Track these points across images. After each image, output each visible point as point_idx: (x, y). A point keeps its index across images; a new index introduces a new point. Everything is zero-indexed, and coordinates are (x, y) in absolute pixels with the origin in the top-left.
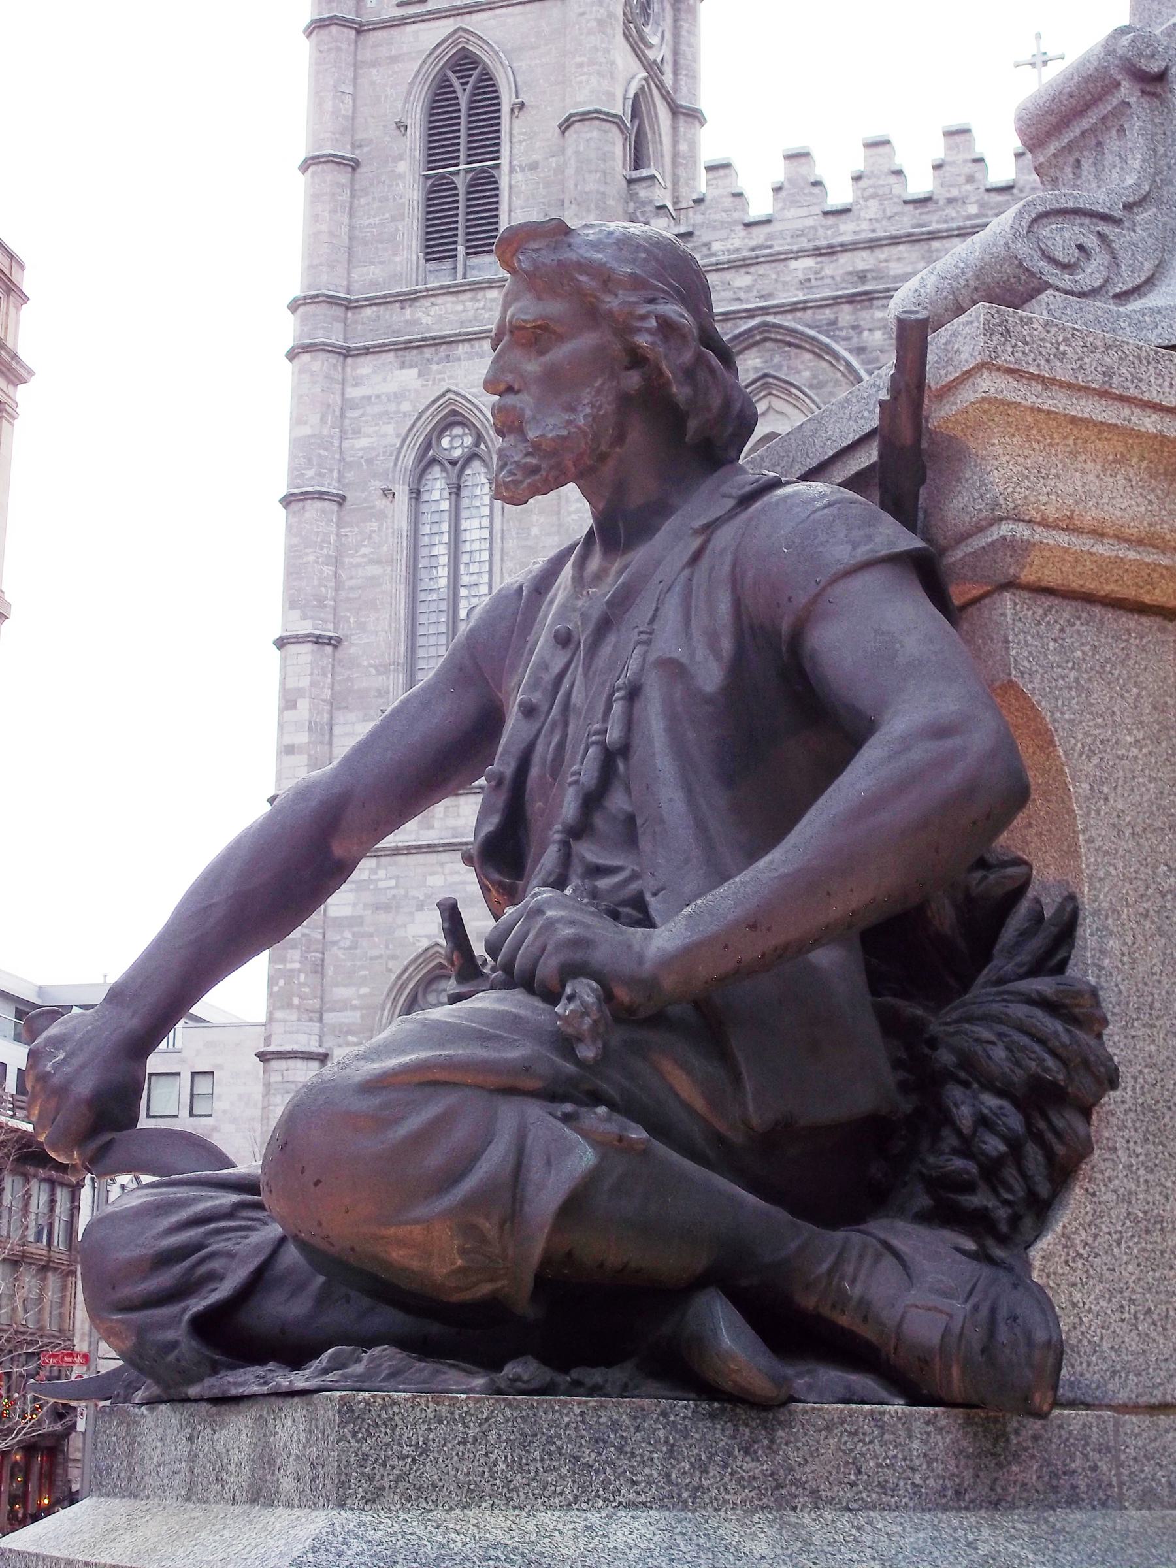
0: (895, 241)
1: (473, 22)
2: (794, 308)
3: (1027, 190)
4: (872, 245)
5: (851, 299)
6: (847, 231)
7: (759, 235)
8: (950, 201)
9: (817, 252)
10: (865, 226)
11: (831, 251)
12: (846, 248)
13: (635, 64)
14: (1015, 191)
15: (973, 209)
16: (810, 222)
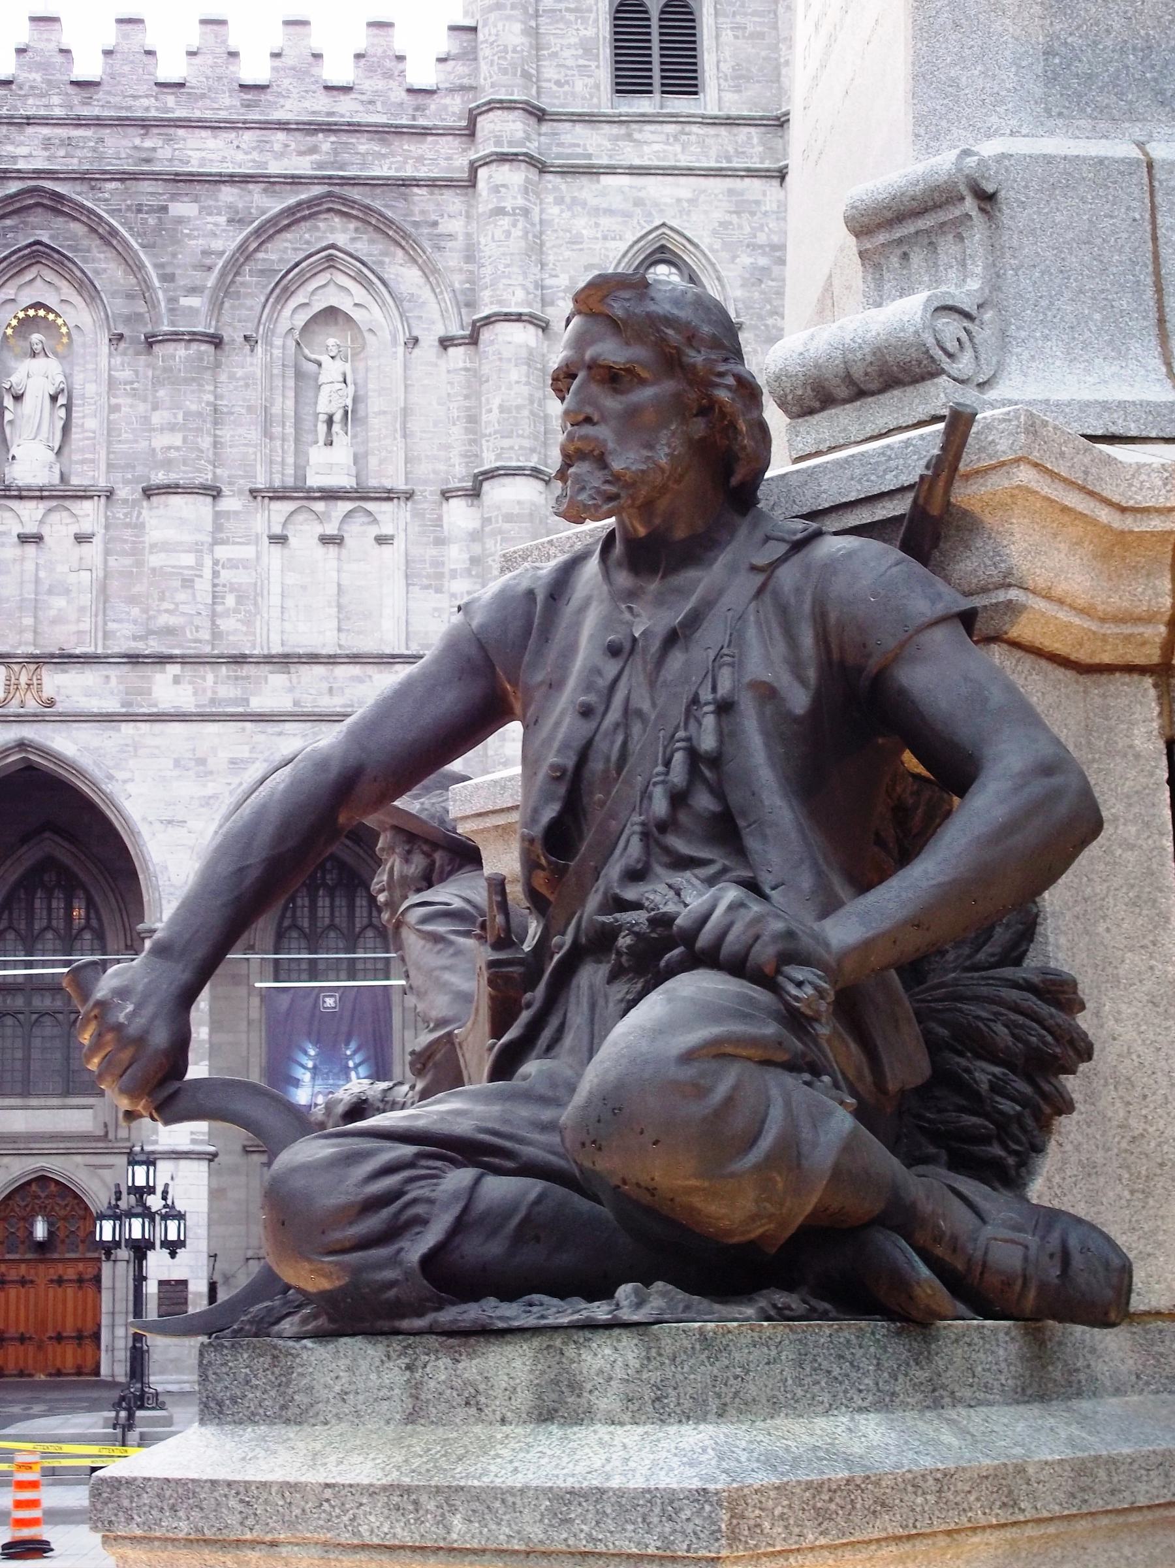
3: (26, 87)
14: (14, 87)
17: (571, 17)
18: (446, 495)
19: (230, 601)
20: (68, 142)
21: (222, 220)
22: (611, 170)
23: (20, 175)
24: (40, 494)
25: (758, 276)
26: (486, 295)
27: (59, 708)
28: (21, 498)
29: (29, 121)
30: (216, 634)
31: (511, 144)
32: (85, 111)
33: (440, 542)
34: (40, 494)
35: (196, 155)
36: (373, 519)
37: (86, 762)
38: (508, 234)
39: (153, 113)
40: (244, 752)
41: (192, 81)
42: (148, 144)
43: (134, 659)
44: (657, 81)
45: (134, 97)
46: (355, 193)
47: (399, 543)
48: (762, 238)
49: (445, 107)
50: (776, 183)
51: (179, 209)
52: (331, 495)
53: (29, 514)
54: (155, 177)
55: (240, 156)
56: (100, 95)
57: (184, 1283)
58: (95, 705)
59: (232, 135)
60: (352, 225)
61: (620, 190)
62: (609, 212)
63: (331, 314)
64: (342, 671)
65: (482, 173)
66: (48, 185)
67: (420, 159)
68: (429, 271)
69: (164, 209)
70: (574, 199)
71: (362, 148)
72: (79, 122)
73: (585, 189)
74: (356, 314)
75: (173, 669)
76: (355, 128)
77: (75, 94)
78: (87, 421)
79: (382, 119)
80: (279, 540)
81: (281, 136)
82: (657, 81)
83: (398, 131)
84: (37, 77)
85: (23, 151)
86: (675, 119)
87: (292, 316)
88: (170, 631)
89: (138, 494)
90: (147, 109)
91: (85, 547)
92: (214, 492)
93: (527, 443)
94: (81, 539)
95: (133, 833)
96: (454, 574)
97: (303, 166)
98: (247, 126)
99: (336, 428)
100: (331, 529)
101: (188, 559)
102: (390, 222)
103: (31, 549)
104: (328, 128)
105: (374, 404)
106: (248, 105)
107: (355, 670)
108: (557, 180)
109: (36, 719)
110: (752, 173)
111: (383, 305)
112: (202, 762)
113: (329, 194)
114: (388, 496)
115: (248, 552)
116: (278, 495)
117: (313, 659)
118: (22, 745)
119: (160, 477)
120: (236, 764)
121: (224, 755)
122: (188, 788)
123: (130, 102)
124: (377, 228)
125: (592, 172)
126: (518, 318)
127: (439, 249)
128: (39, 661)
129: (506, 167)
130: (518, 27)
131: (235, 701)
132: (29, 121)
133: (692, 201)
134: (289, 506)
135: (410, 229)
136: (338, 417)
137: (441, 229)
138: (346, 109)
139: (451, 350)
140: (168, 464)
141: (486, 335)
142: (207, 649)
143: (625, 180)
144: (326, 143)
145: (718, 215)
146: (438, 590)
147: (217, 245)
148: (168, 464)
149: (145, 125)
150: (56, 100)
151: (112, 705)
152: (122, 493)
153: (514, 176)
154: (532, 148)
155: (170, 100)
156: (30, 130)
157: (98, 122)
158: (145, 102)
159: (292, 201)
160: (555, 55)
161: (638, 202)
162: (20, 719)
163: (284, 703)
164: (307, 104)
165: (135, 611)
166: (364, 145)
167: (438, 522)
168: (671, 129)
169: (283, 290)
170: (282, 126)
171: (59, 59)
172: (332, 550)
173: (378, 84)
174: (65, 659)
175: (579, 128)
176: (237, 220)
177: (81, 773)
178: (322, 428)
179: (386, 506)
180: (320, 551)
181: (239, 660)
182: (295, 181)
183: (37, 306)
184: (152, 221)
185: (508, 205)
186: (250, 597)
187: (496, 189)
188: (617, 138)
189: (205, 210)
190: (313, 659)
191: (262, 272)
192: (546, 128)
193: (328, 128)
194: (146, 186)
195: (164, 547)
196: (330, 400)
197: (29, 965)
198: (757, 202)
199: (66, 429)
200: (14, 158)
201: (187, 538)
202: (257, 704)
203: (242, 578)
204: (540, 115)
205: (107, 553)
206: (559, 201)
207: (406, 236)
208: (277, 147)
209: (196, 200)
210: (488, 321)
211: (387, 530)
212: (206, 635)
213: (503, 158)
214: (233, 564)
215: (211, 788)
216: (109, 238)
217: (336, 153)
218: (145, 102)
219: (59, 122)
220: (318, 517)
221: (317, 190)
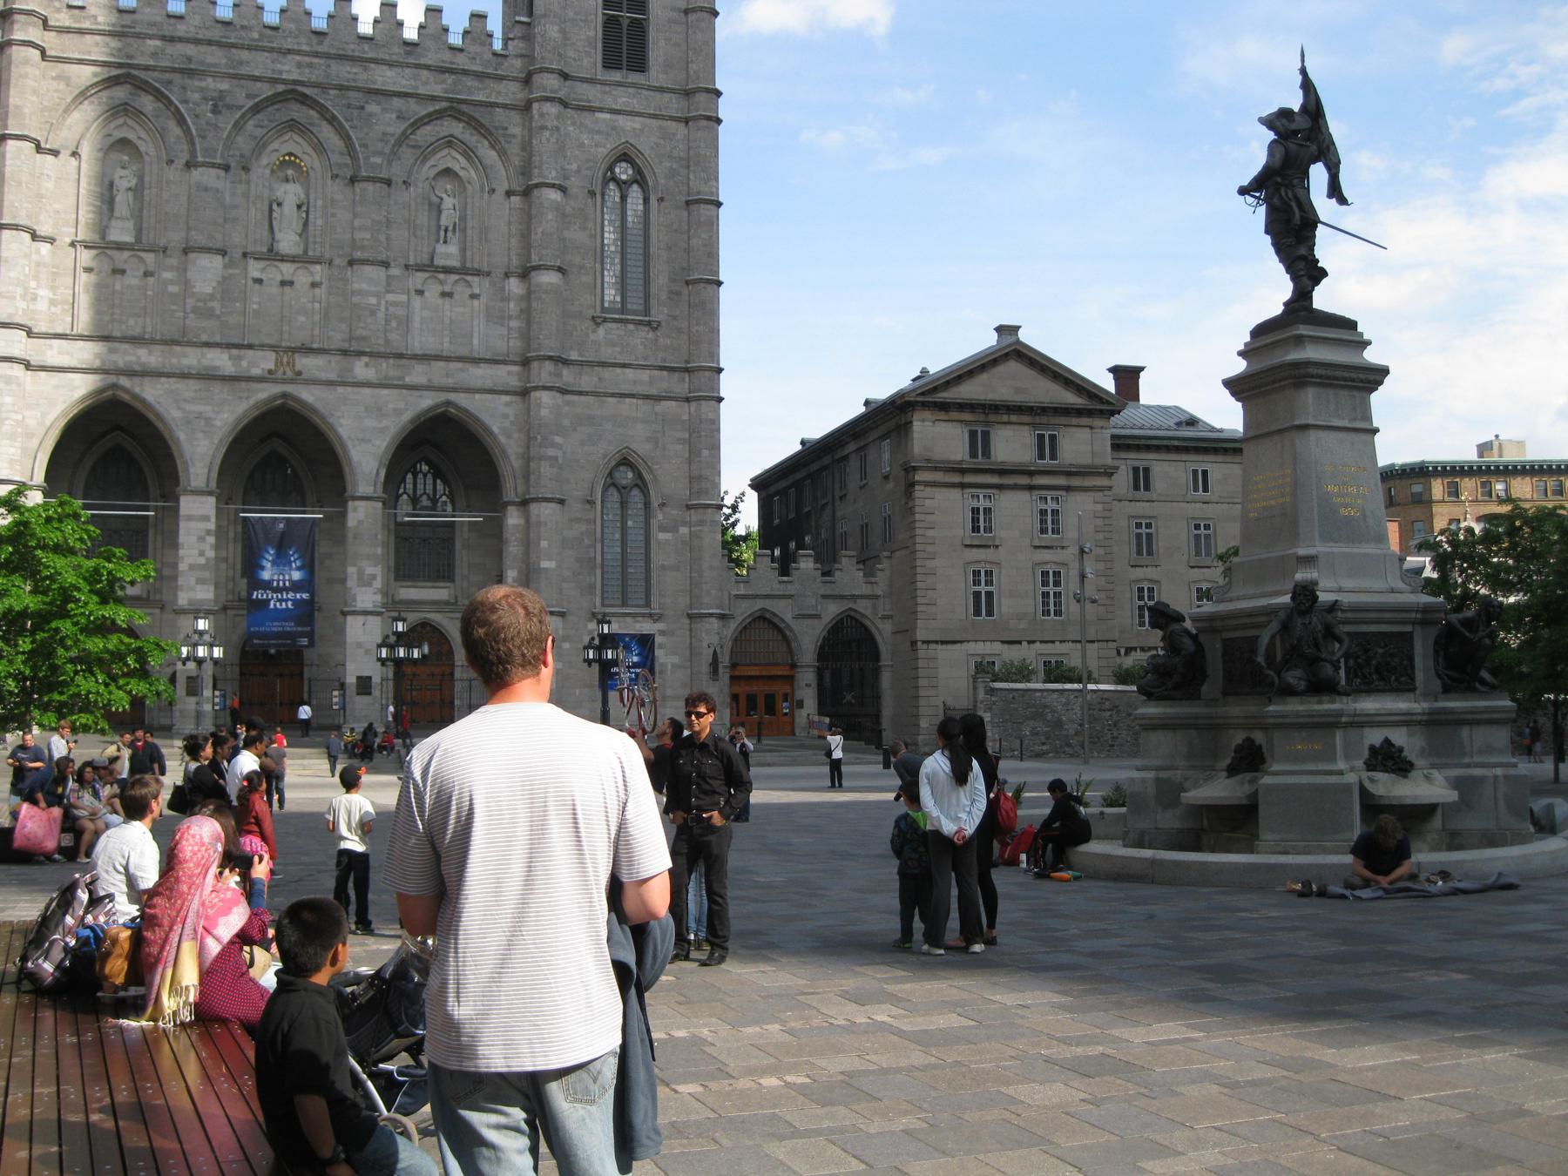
0: (210, 43)
2: (147, 68)
4: (197, 42)
5: (182, 71)
6: (181, 29)
7: (128, 19)
8: (243, 27)
9: (164, 38)
10: (192, 29)
11: (171, 40)
12: (181, 40)
15: (256, 36)
16: (159, 19)
17: (582, 24)
18: (507, 275)
19: (394, 324)
20: (310, 65)
21: (394, 116)
22: (601, 110)
23: (284, 82)
24: (293, 259)
25: (673, 173)
26: (536, 171)
27: (305, 376)
28: (282, 261)
29: (290, 52)
30: (387, 341)
31: (551, 92)
32: (320, 49)
34: (293, 259)
35: (380, 79)
36: (469, 285)
37: (318, 405)
38: (548, 140)
39: (357, 54)
40: (401, 405)
41: (378, 37)
42: (354, 70)
43: (345, 353)
44: (625, 63)
45: (347, 43)
46: (465, 108)
47: (484, 299)
48: (675, 153)
49: (513, 66)
50: (683, 124)
51: (372, 108)
52: (448, 270)
53: (287, 269)
54: (358, 89)
55: (404, 82)
56: (327, 41)
57: (370, 678)
58: (324, 376)
59: (400, 70)
60: (461, 125)
61: (605, 120)
62: (599, 132)
63: (447, 172)
64: (454, 365)
65: (535, 105)
66: (300, 88)
67: (499, 93)
68: (502, 154)
69: (363, 108)
70: (581, 124)
71: (469, 84)
72: (316, 55)
73: (587, 118)
74: (462, 173)
75: (365, 359)
76: (465, 72)
77: (314, 39)
78: (317, 220)
79: (480, 69)
80: (420, 292)
81: (425, 73)
82: (625, 63)
83: (488, 76)
84: (292, 26)
85: (286, 68)
86: (634, 85)
87: (427, 171)
88: (364, 339)
89: (345, 263)
90: (353, 51)
91: (317, 291)
92: (386, 264)
93: (556, 253)
95: (343, 446)
96: (510, 317)
97: (437, 89)
98: (408, 65)
99: (450, 234)
100: (447, 289)
101: (373, 300)
102: (483, 126)
103: (287, 289)
104: (451, 71)
106: (408, 53)
107: (461, 365)
108: (573, 112)
109: (292, 381)
110: (672, 118)
111: (476, 170)
112: (380, 409)
113: (452, 108)
114: (478, 273)
115: (404, 298)
116: (420, 268)
117: (438, 358)
118: (285, 395)
119: (358, 254)
120: (398, 412)
121: (391, 406)
122: (371, 423)
123: (345, 46)
124: (475, 128)
126: (553, 186)
127: (509, 142)
128: (294, 350)
129: (548, 104)
130: (556, 28)
131: (399, 379)
132: (290, 52)
133: (642, 130)
134: (426, 275)
135: (493, 131)
136: (451, 228)
137: (509, 132)
138: (461, 61)
139: (513, 198)
140: (362, 248)
141: (536, 192)
142: (382, 349)
143: (607, 116)
144: (450, 79)
145: (653, 139)
146: (502, 325)
147: (390, 130)
148: (362, 248)
149: (352, 59)
150: (303, 40)
151: (332, 376)
152: (337, 261)
153: (551, 109)
154: (561, 94)
155: (366, 47)
156: (290, 57)
157: (327, 56)
158: (352, 46)
159: (431, 109)
160: (573, 44)
161: (614, 128)
162: (284, 381)
163: (423, 380)
164: (439, 56)
165: (344, 326)
166: (470, 82)
167: (503, 289)
168: (631, 90)
169: (424, 156)
170: (427, 67)
171: (304, 18)
172: (447, 300)
173: (477, 48)
174: (307, 350)
175: (585, 85)
176: (401, 117)
177: (316, 411)
178: (442, 233)
179: (476, 279)
180: (440, 301)
181: (400, 356)
182: (433, 98)
183: (290, 154)
184: (356, 113)
185: (549, 124)
186: (406, 322)
187: (542, 115)
188: (605, 93)
189: (385, 110)
190: (438, 358)
191: (414, 147)
192: (568, 83)
193: (451, 71)
194: (352, 94)
195: (360, 292)
197: (304, 513)
198: (674, 134)
199: (306, 224)
200: (281, 72)
201: (373, 289)
202: (408, 380)
203: (401, 312)
204: (565, 76)
205: (329, 293)
206: (573, 124)
207: (491, 134)
208: (424, 79)
209: (379, 104)
210: (537, 186)
211: (477, 291)
212: (381, 342)
213: (548, 99)
214: (395, 304)
215: (385, 423)
216: (332, 120)
217: (455, 83)
218: (352, 46)
219: (306, 54)
220: (441, 282)
221: (445, 104)
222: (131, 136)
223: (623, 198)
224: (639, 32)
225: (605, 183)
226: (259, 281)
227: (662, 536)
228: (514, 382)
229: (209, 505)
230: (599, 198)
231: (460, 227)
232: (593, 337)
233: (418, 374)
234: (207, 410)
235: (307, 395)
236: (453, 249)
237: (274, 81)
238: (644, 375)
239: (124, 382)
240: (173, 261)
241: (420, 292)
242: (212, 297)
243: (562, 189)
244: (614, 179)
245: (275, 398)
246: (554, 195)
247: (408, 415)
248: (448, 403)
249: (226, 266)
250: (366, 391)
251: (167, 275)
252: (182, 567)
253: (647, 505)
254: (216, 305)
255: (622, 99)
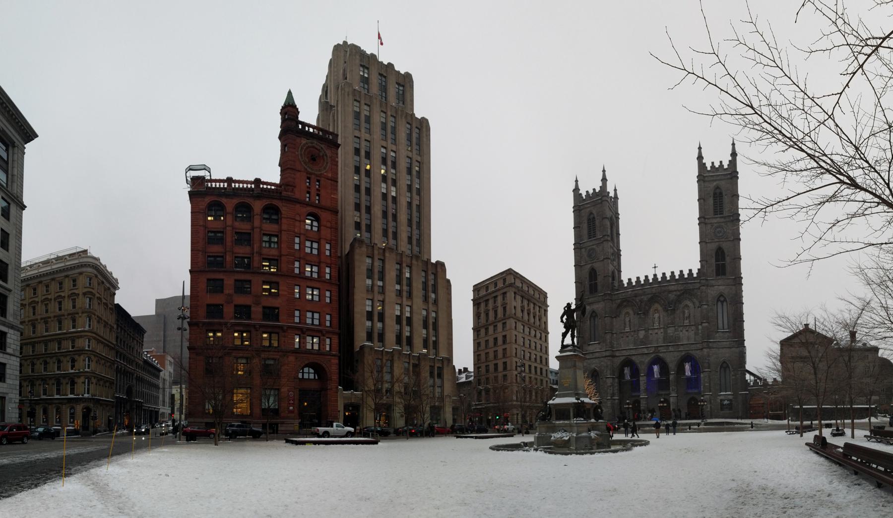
1: (593, 264)
13: (612, 267)
33: (698, 330)
36: (691, 328)
53: (656, 331)
63: (686, 305)
80: (682, 331)
92: (675, 327)
94: (662, 333)
97: (682, 288)
101: (672, 334)
105: (691, 315)
114: (693, 325)
115: (678, 333)
120: (678, 356)
125: (713, 286)
143: (717, 287)
162: (657, 353)
176: (675, 295)
182: (681, 290)
195: (669, 333)
196: (686, 315)
210: (701, 305)
222: (627, 311)
223: (722, 305)
224: (724, 266)
225: (718, 301)
226: (651, 334)
227: (733, 377)
228: (701, 347)
229: (645, 378)
230: (716, 306)
231: (689, 316)
232: (716, 336)
233: (681, 349)
234: (643, 360)
235: (661, 355)
236: (687, 321)
237: (651, 294)
238: (728, 343)
239: (629, 357)
240: (636, 333)
241: (682, 331)
242: (643, 338)
243: (708, 305)
244: (719, 300)
245: (654, 356)
246: (706, 306)
247: (679, 357)
248: (688, 353)
249: (645, 332)
250: (672, 353)
251: (635, 336)
252: (641, 390)
253: (730, 370)
254: (644, 340)
255: (720, 282)
